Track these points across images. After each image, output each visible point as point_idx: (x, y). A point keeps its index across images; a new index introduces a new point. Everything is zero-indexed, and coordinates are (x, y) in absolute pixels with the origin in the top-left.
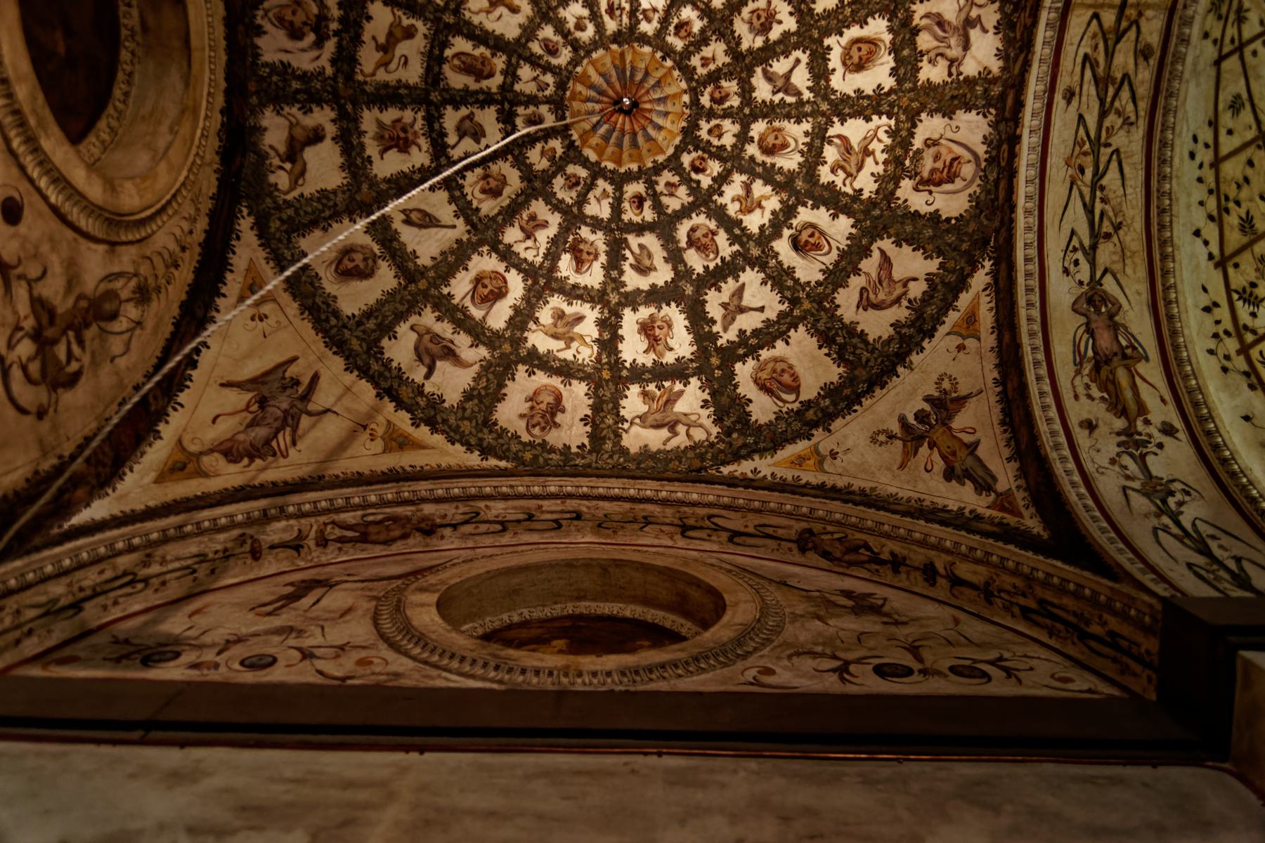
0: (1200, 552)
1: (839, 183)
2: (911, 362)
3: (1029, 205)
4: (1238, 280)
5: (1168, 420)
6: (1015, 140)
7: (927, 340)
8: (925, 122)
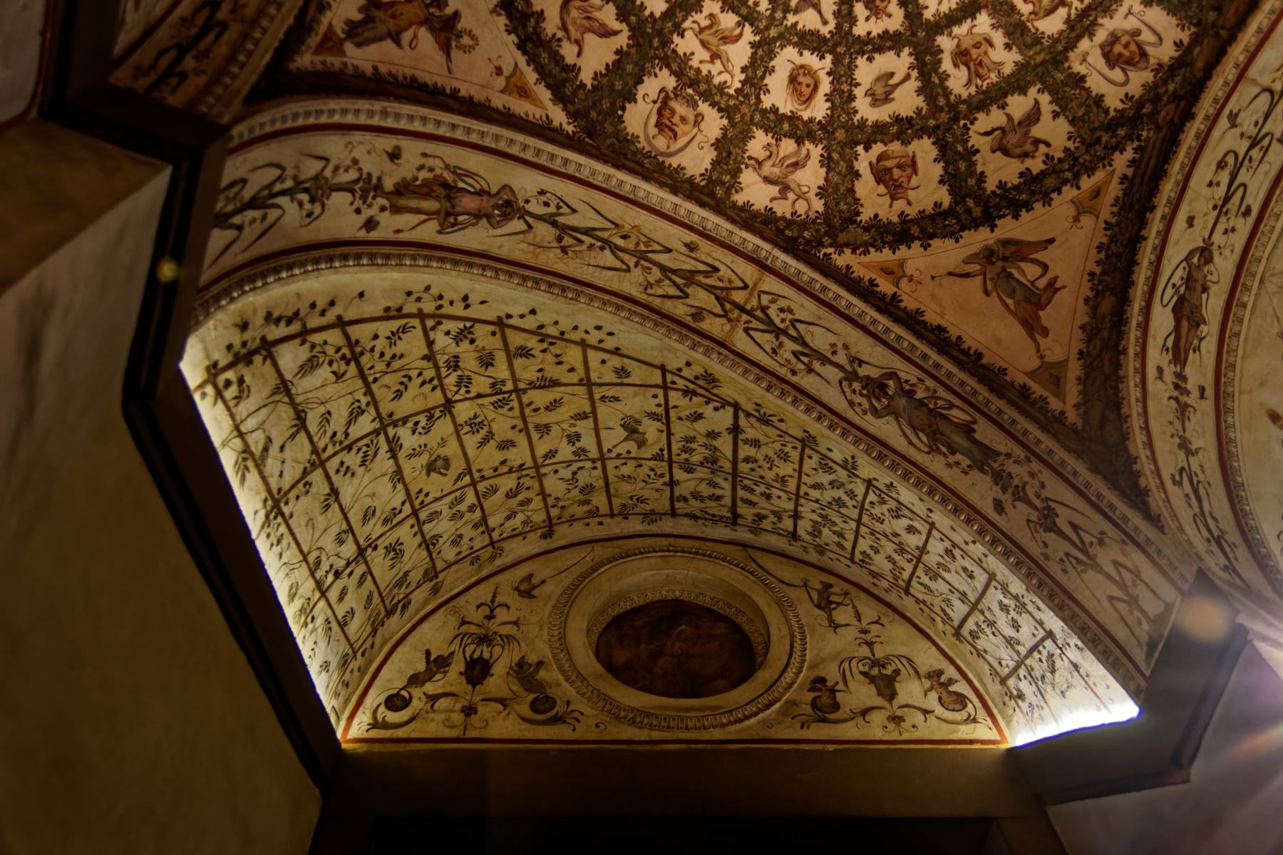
0: (254, 199)
1: (697, 17)
2: (499, 15)
3: (614, 182)
4: (481, 331)
5: (380, 228)
6: (674, 191)
7: (516, 41)
8: (719, 121)
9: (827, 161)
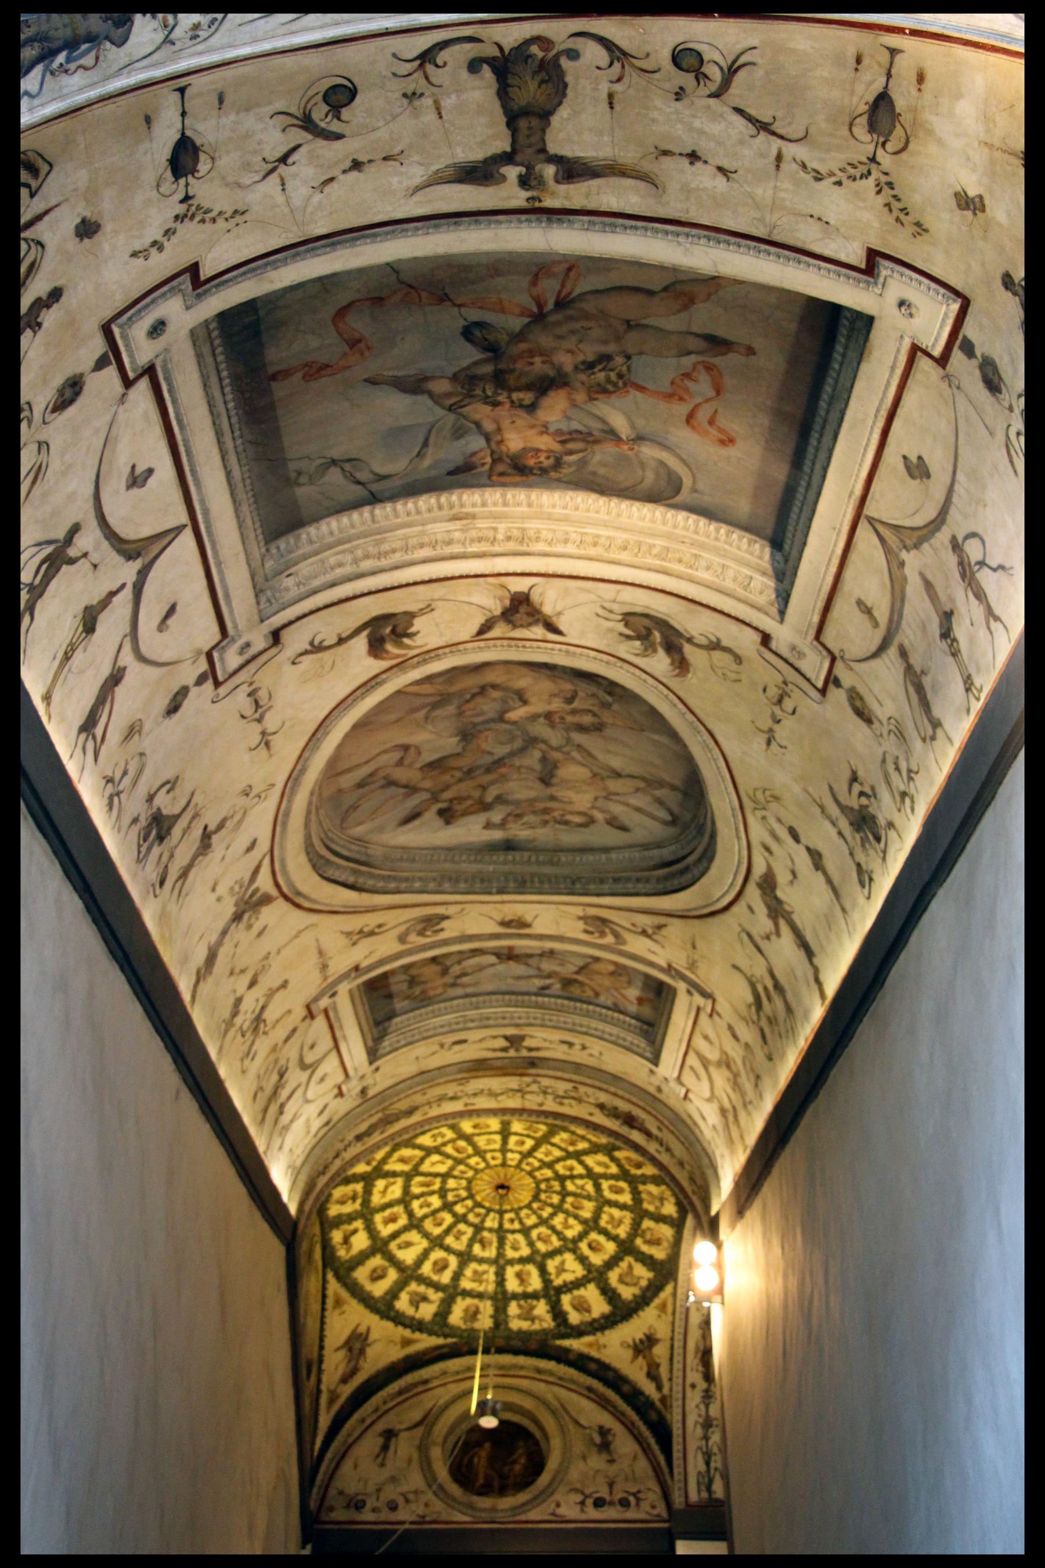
9: (644, 1183)
